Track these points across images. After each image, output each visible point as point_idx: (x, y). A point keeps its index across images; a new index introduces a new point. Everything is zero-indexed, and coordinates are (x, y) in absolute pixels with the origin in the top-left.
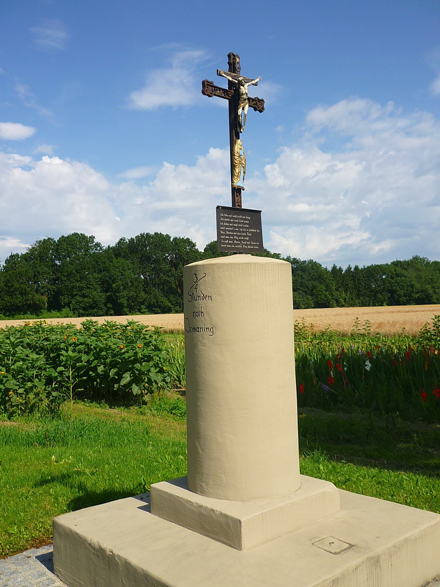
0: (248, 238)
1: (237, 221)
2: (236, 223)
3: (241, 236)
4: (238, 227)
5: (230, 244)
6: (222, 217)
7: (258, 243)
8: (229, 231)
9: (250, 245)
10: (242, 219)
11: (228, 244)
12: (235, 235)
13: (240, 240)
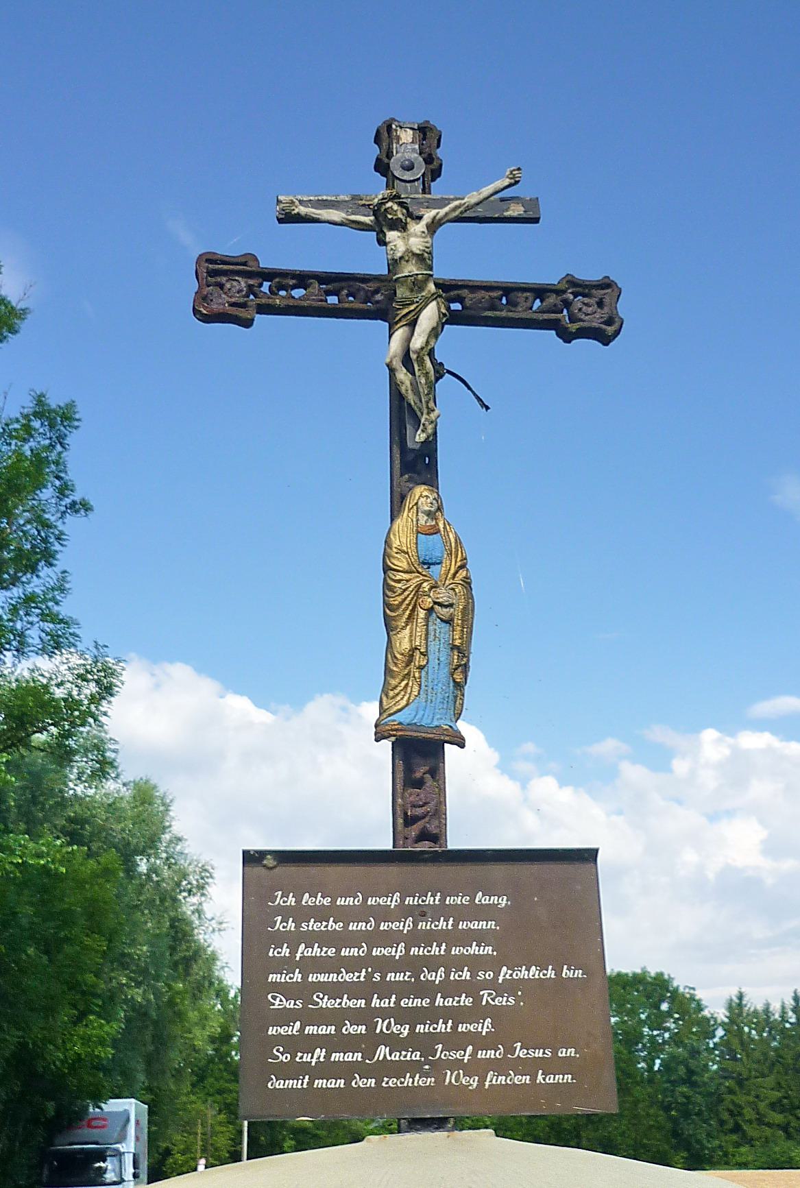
0: (485, 1027)
1: (406, 926)
2: (390, 939)
3: (433, 1014)
4: (413, 965)
5: (347, 1071)
6: (286, 913)
8: (334, 991)
9: (500, 1067)
12: (384, 1013)
13: (425, 1044)
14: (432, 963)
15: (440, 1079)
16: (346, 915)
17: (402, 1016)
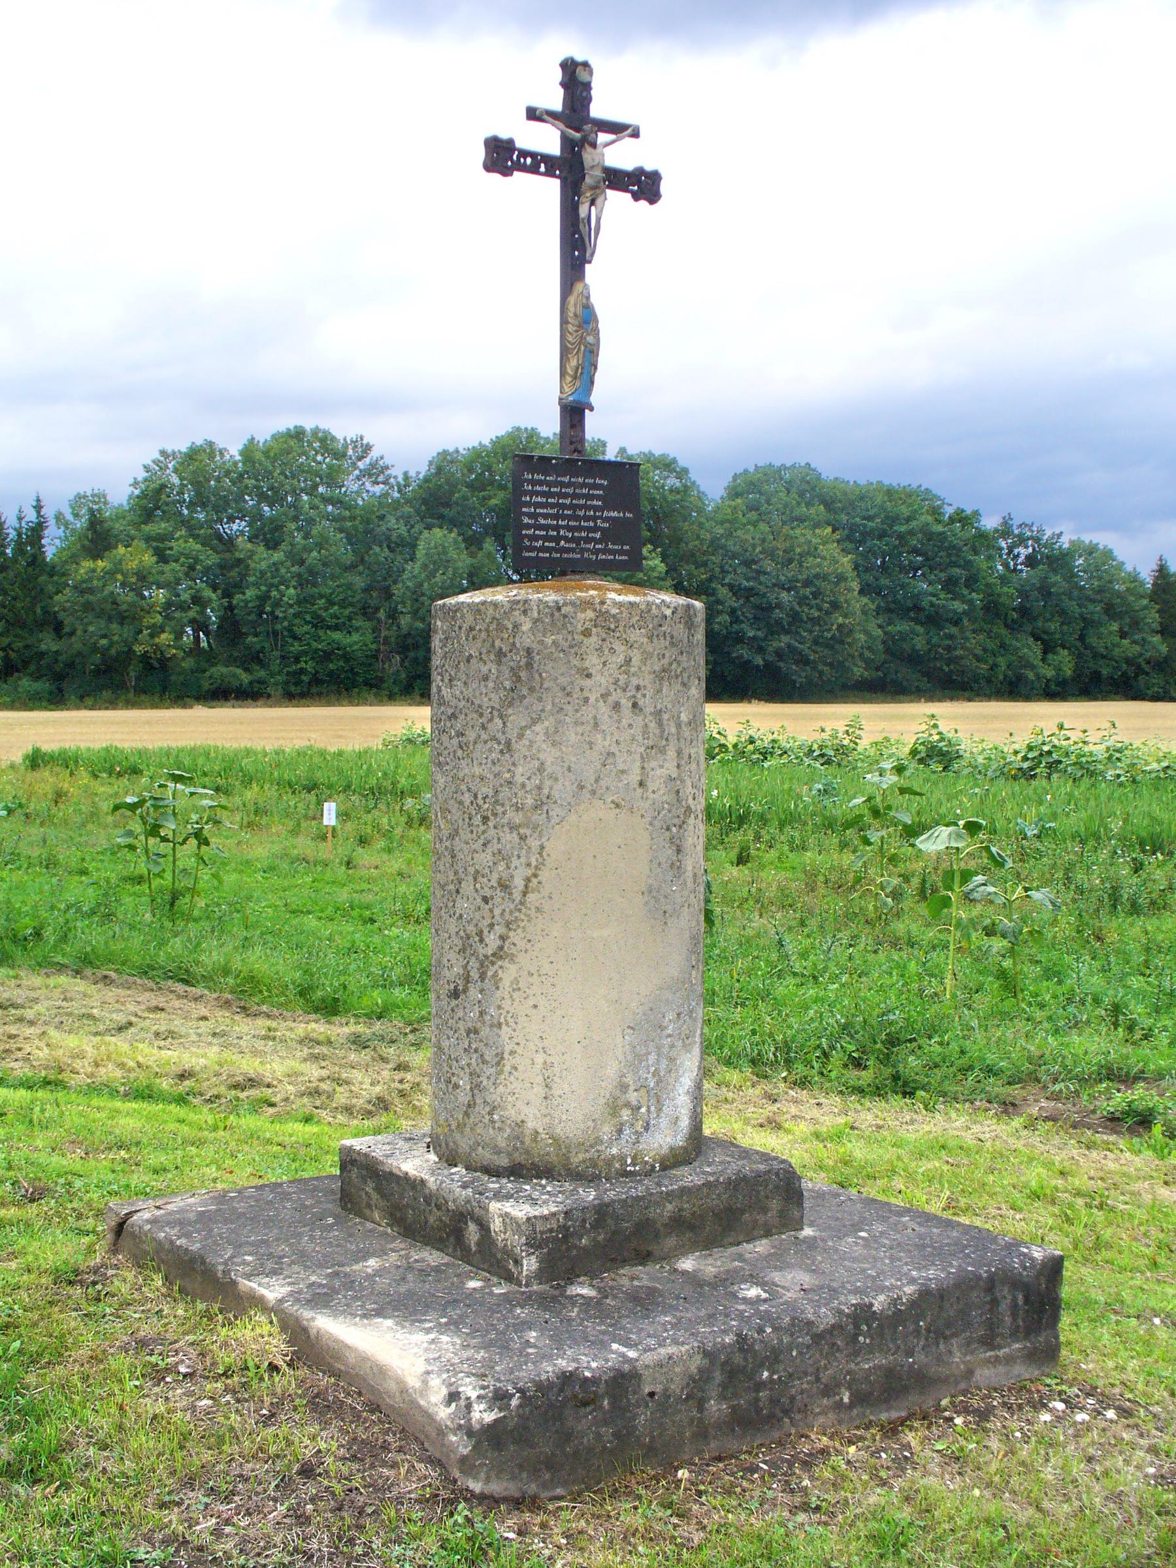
0: (598, 535)
1: (570, 491)
3: (580, 529)
4: (573, 507)
5: (549, 550)
7: (626, 547)
8: (545, 516)
9: (604, 551)
10: (584, 485)
11: (543, 549)
12: (563, 527)
14: (581, 507)
15: (582, 555)
16: (549, 484)
17: (569, 528)
